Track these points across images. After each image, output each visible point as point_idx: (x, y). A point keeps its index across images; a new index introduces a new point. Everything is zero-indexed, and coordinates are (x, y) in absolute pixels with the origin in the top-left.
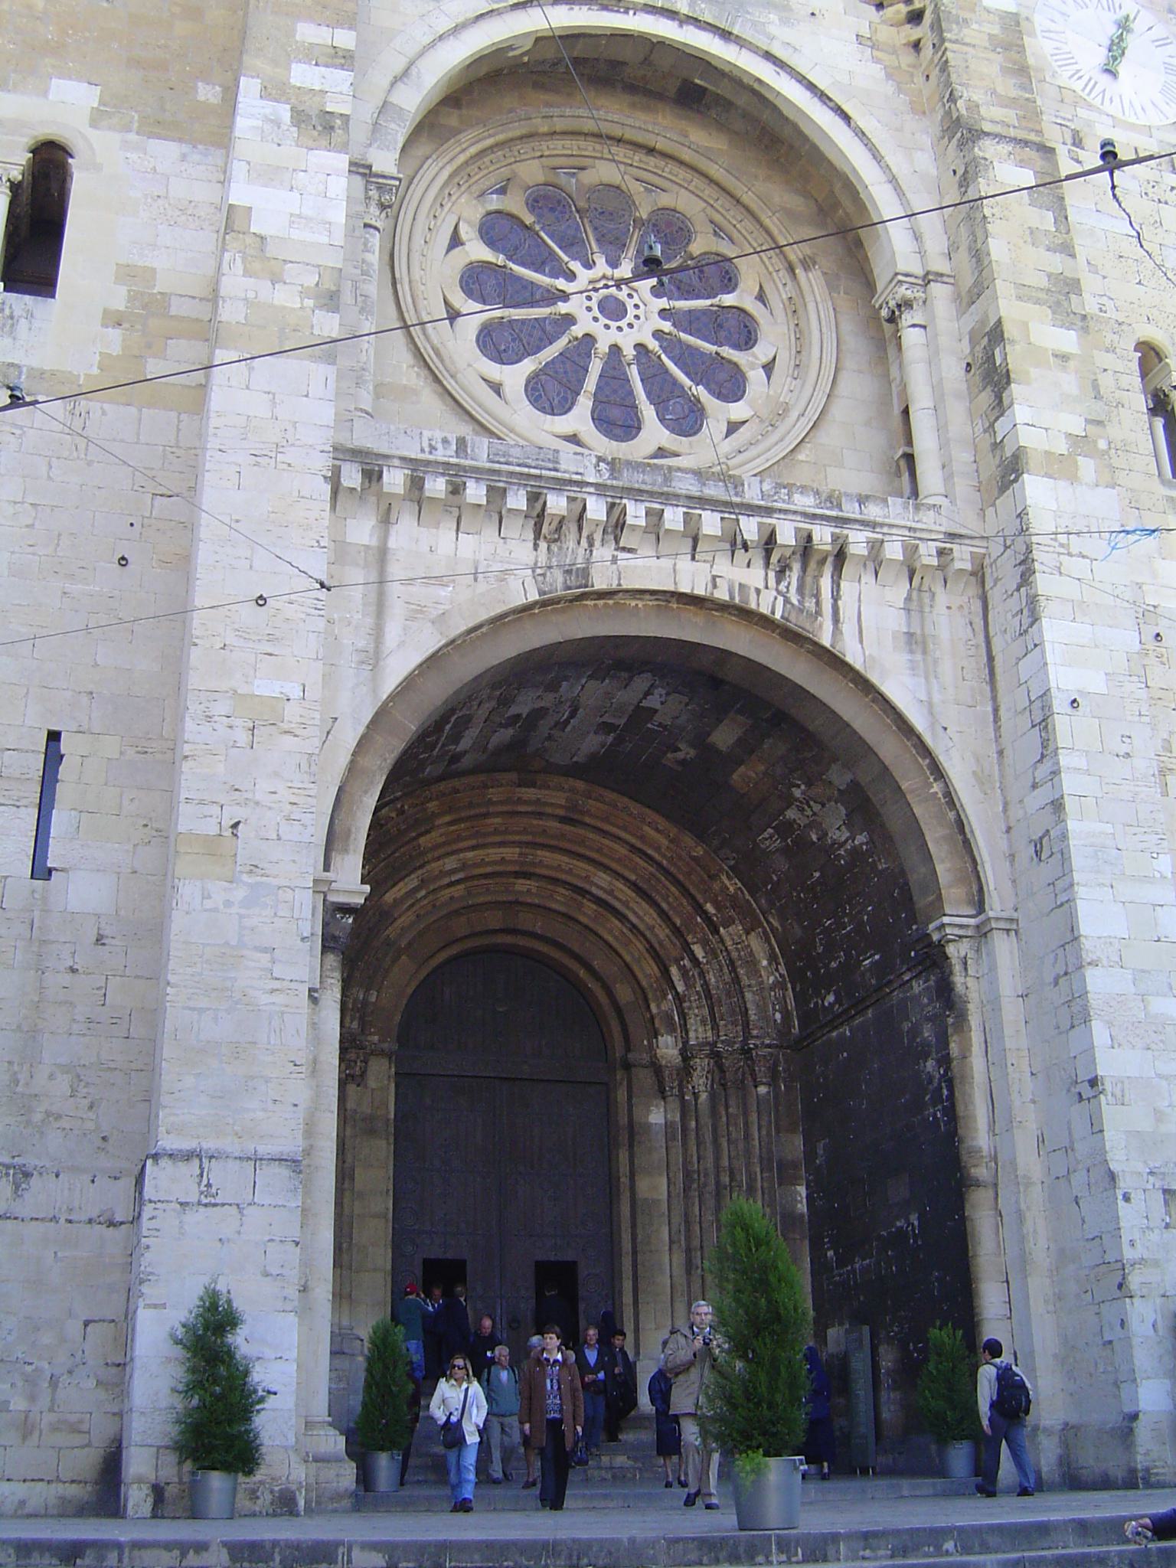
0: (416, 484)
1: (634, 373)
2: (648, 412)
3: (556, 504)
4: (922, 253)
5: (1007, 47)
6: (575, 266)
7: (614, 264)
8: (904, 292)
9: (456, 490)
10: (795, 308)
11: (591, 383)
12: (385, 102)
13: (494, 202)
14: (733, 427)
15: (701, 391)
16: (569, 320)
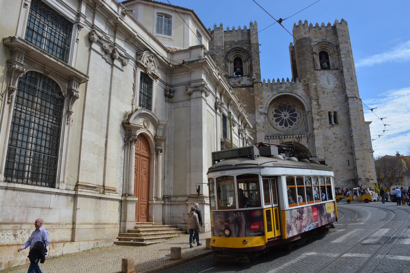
0: (271, 137)
1: (287, 121)
2: (288, 124)
3: (280, 137)
4: (308, 109)
5: (315, 89)
6: (282, 113)
7: (285, 112)
8: (307, 113)
9: (273, 137)
10: (300, 112)
11: (284, 123)
12: (266, 107)
13: (275, 108)
14: (295, 124)
15: (292, 121)
16: (282, 117)
